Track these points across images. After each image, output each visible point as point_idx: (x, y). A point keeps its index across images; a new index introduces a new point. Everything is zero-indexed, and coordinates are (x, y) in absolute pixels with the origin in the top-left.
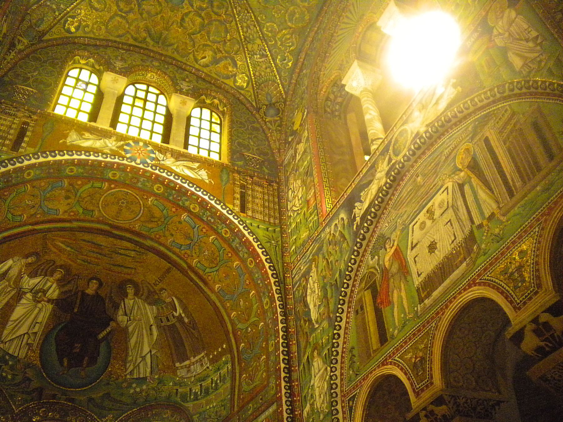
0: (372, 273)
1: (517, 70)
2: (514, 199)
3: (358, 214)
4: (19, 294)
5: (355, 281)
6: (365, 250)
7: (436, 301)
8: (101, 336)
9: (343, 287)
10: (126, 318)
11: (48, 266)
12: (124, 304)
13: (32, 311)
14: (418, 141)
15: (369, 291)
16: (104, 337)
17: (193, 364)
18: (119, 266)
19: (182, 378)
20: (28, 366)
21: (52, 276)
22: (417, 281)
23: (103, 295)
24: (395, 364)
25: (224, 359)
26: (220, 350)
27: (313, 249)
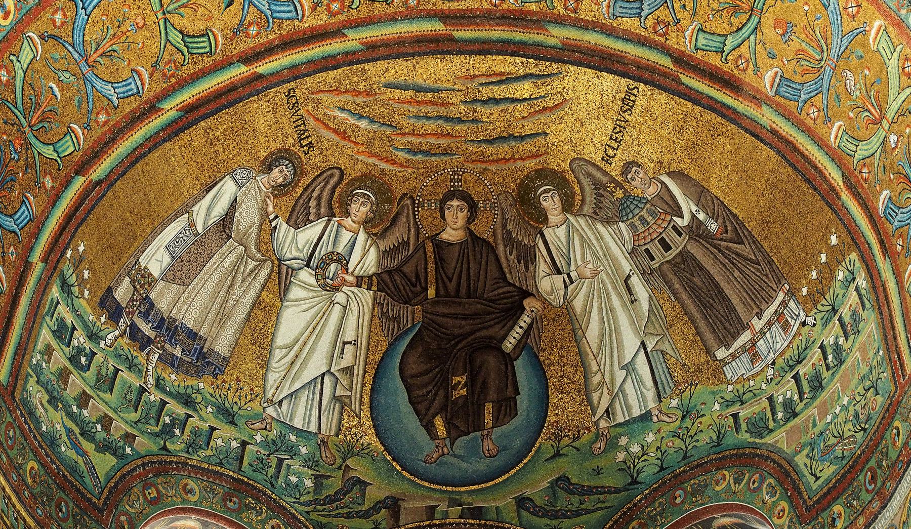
4: (279, 274)
8: (509, 344)
10: (558, 280)
11: (329, 186)
12: (546, 243)
13: (324, 314)
16: (519, 341)
17: (762, 333)
18: (501, 139)
19: (743, 380)
20: (349, 451)
21: (347, 214)
23: (487, 236)
25: (840, 276)
26: (823, 258)
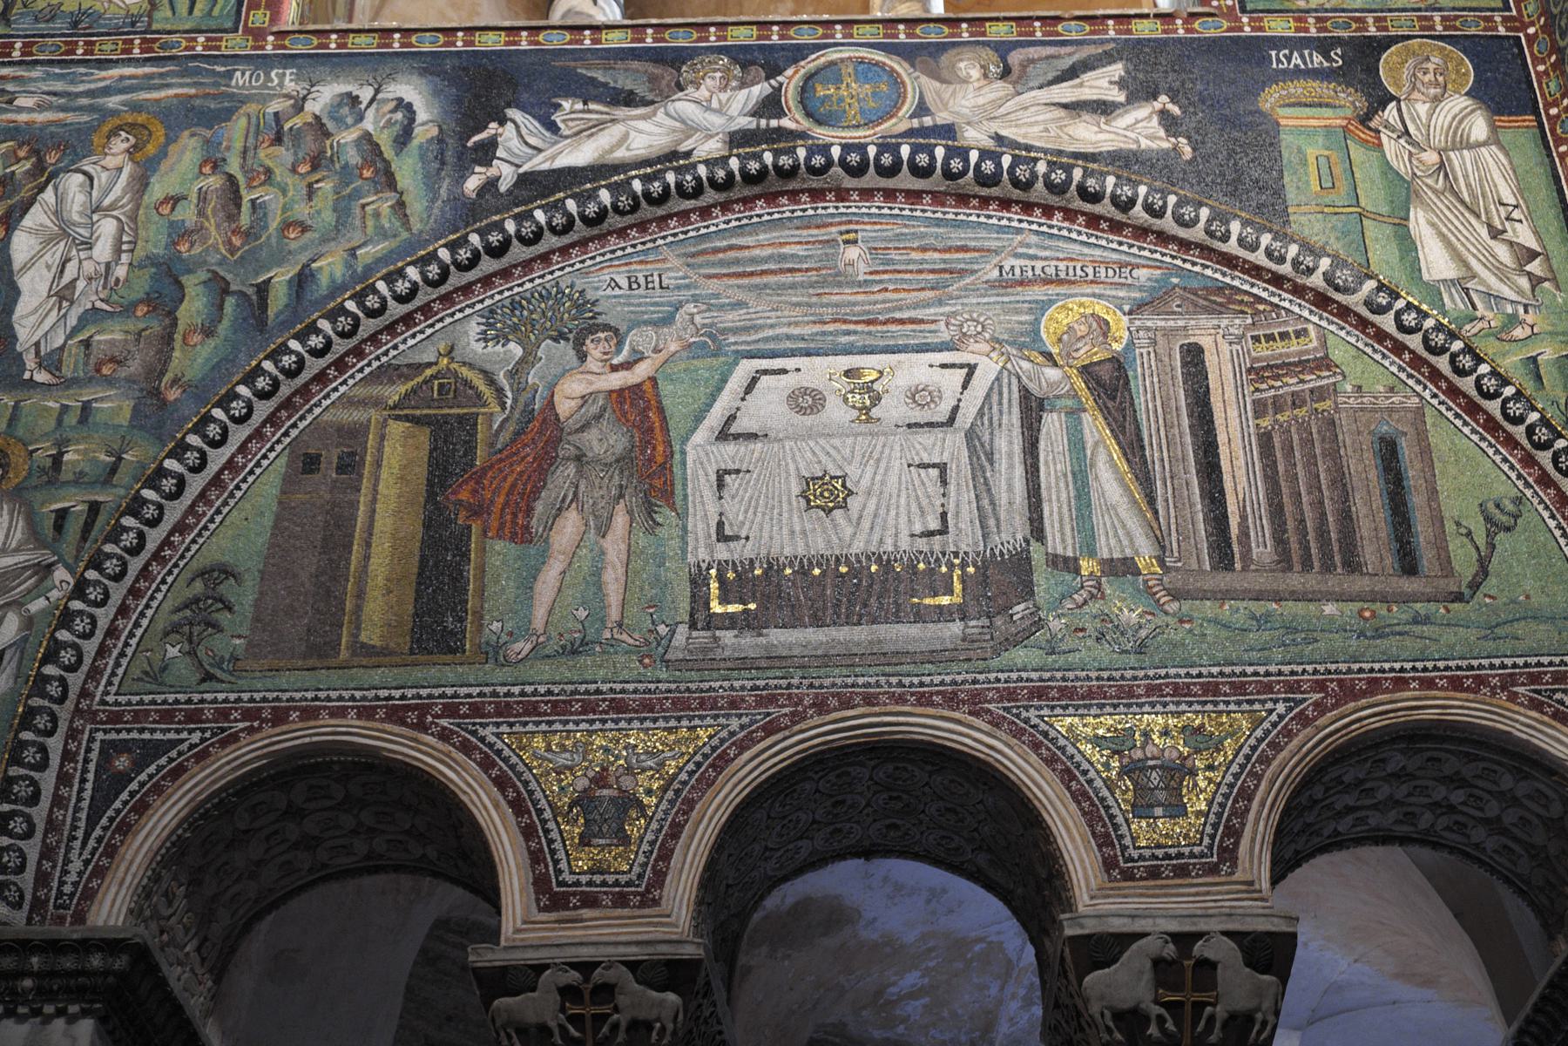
0: (467, 384)
1: (1426, 277)
2: (1224, 580)
3: (508, 150)
5: (358, 352)
6: (466, 290)
7: (775, 660)
9: (302, 337)
14: (940, 152)
15: (424, 437)
22: (702, 550)
24: (466, 748)
27: (146, 83)
